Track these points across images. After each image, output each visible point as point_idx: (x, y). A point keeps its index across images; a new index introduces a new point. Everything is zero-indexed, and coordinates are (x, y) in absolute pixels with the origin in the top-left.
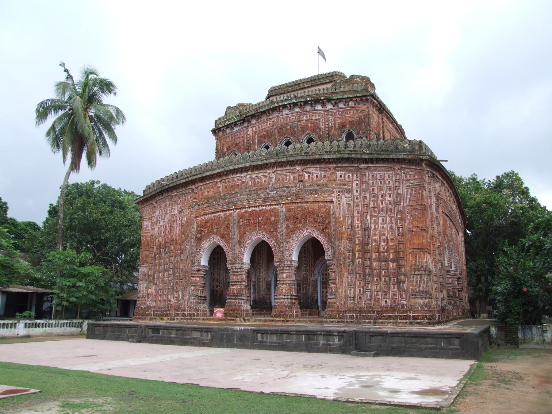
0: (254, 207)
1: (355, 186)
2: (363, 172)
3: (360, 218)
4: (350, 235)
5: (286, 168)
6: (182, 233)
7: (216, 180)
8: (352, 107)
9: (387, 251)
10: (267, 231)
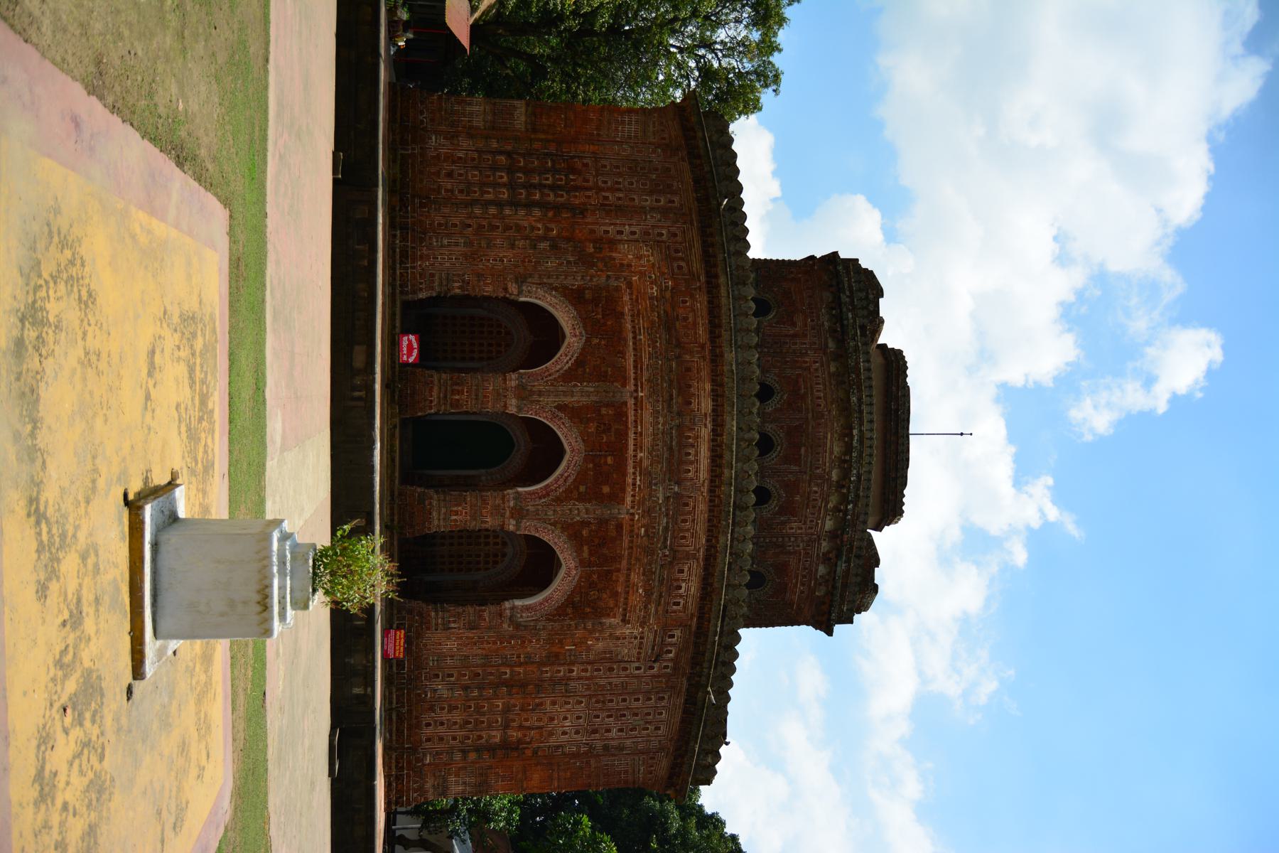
9: (521, 727)
10: (581, 477)
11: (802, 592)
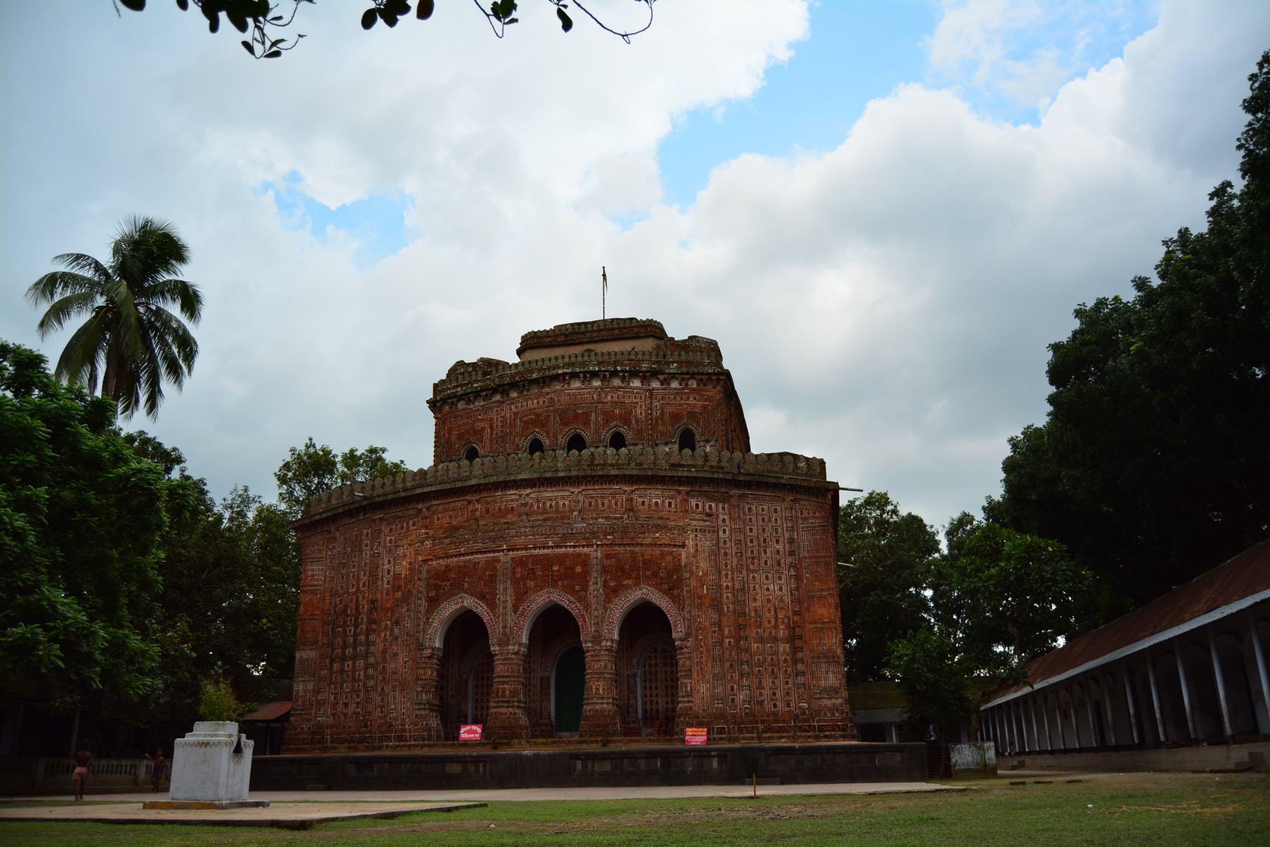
1: (720, 522)
2: (732, 501)
4: (714, 600)
6: (396, 588)
8: (694, 389)
9: (776, 627)
10: (569, 590)
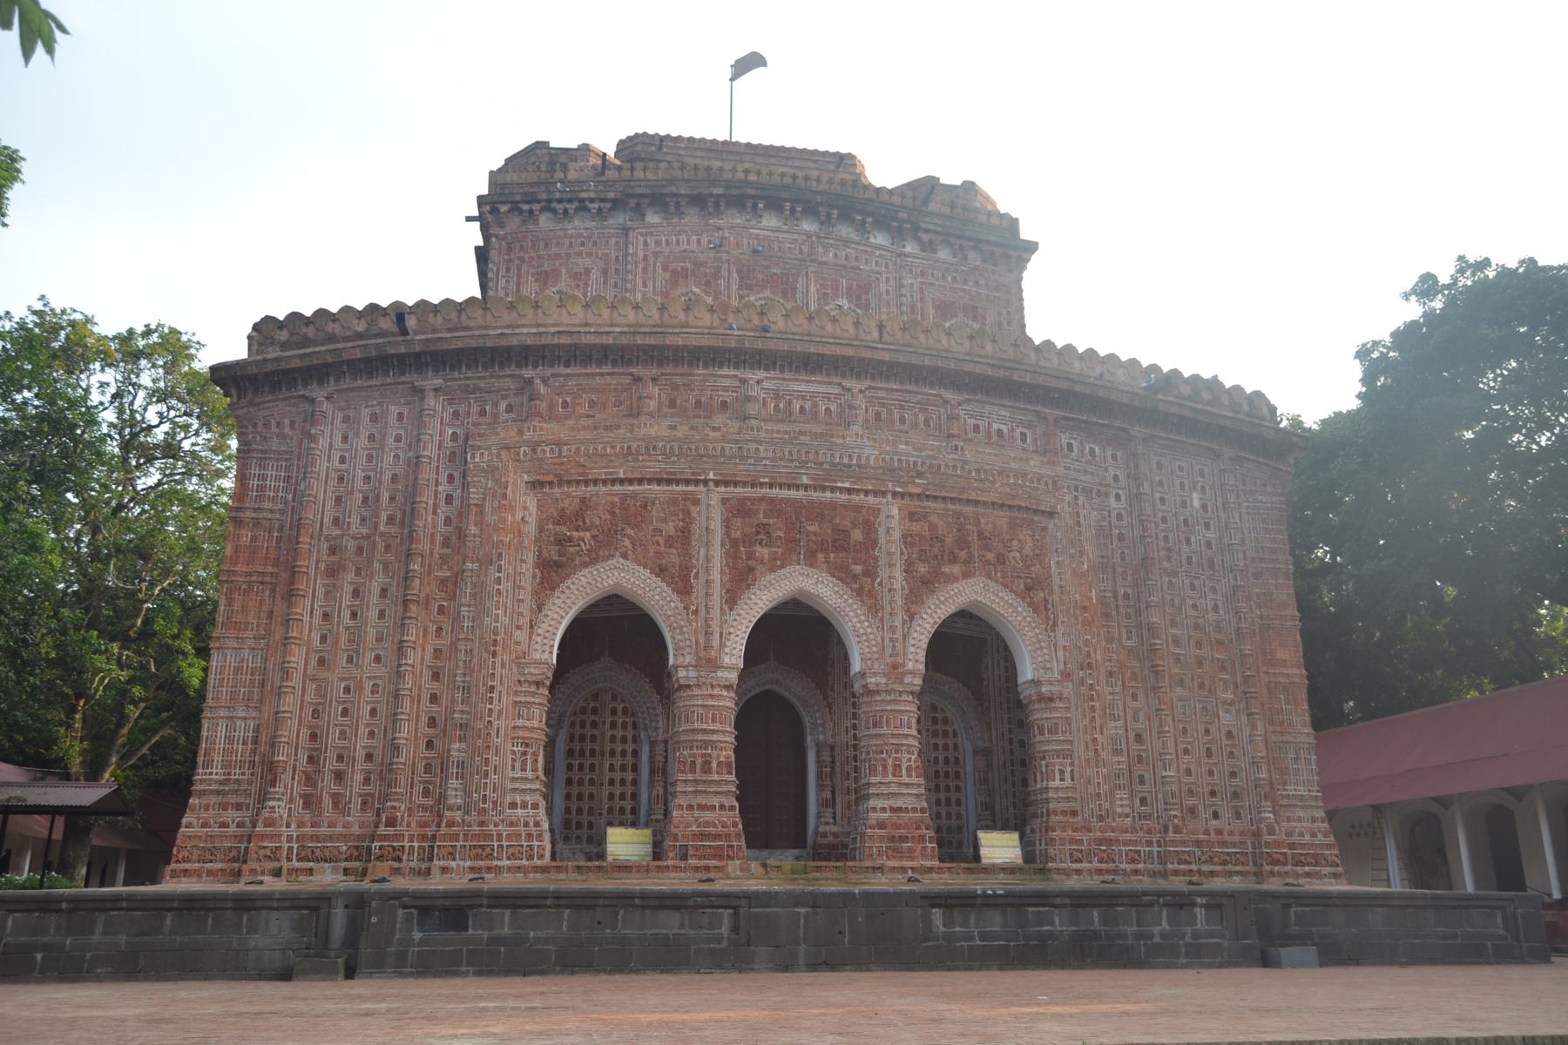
0: (789, 487)
3: (1130, 572)
5: (908, 387)
7: (637, 370)
10: (841, 573)
11: (977, 284)
